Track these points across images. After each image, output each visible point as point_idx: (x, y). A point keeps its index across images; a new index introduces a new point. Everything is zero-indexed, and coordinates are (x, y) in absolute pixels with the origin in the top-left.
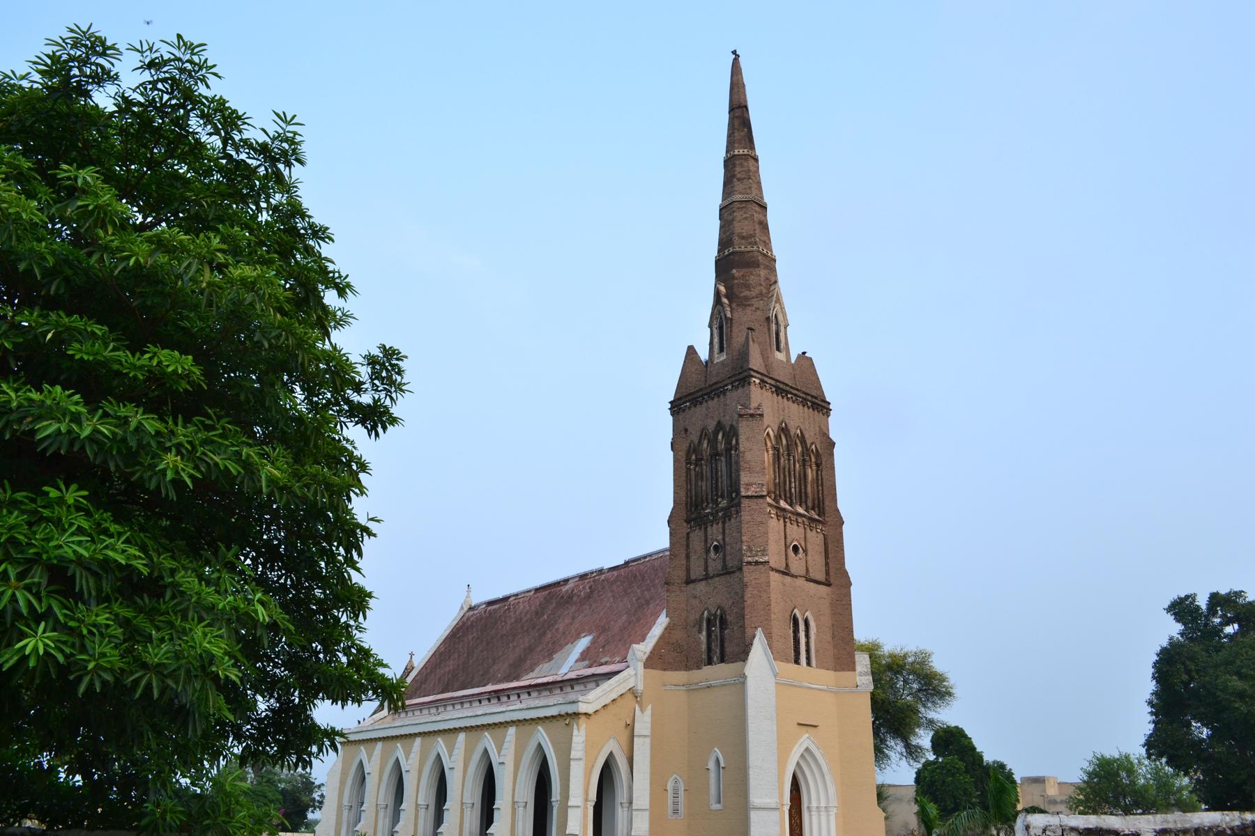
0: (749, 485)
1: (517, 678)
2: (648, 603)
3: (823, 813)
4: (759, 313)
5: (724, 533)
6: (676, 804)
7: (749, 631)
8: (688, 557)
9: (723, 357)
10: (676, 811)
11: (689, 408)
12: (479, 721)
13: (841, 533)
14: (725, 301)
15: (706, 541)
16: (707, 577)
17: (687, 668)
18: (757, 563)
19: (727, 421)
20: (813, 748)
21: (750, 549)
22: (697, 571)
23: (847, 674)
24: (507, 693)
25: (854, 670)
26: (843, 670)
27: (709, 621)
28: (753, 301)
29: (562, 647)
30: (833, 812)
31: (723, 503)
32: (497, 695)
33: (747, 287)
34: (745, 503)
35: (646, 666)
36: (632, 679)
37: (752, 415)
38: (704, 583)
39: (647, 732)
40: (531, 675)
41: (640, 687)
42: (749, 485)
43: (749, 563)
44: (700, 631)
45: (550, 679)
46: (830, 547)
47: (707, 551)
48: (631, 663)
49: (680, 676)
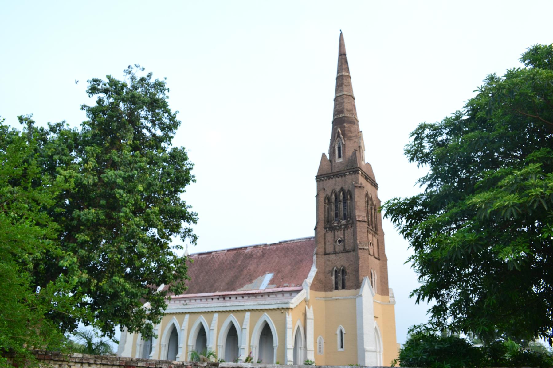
0: (359, 216)
1: (234, 290)
2: (301, 261)
3: (378, 354)
4: (356, 144)
5: (344, 235)
6: (320, 348)
7: (361, 278)
8: (325, 243)
9: (341, 160)
10: (320, 351)
11: (326, 180)
12: (228, 309)
13: (383, 239)
14: (341, 136)
15: (335, 237)
16: (335, 253)
17: (325, 291)
18: (364, 249)
19: (346, 188)
20: (377, 327)
21: (360, 243)
22: (330, 249)
23: (386, 297)
24: (230, 297)
25: (388, 295)
26: (384, 295)
27: (336, 271)
28: (353, 138)
29: (256, 277)
30: (382, 353)
31: (343, 222)
32: (224, 297)
33: (351, 132)
34: (358, 223)
35: (311, 289)
36: (305, 294)
37: (360, 187)
38: (334, 255)
39: (312, 317)
40: (242, 289)
41: (309, 298)
42: (359, 216)
43: (361, 249)
44: (332, 275)
45: (257, 292)
46: (380, 244)
47: (335, 242)
48: (304, 287)
49: (322, 294)
